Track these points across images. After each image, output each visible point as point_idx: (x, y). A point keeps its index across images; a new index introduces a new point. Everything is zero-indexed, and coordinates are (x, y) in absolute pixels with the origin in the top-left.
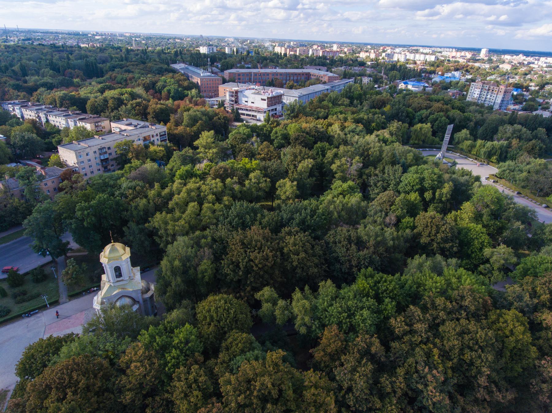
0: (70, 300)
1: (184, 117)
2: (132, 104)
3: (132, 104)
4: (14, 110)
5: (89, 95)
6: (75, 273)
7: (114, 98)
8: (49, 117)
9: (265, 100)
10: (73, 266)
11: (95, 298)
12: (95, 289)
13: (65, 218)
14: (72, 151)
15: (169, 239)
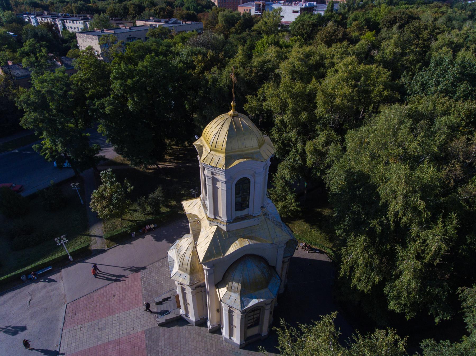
0: (110, 247)
1: (219, 19)
2: (155, 10)
3: (155, 10)
4: (29, 20)
5: (107, 6)
6: (116, 196)
7: (135, 5)
8: (66, 23)
9: (297, 12)
10: (112, 184)
11: (172, 253)
12: (152, 226)
13: (92, 98)
14: (94, 37)
15: (293, 135)
